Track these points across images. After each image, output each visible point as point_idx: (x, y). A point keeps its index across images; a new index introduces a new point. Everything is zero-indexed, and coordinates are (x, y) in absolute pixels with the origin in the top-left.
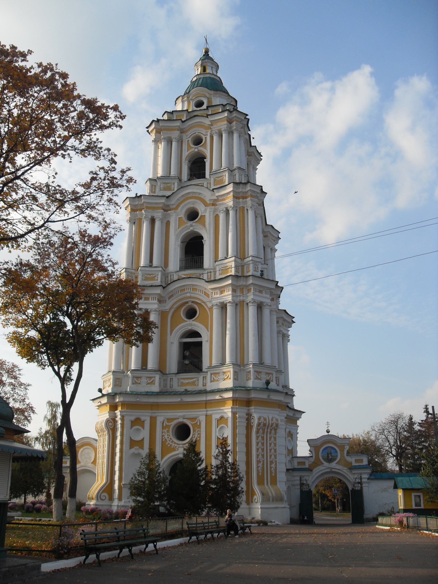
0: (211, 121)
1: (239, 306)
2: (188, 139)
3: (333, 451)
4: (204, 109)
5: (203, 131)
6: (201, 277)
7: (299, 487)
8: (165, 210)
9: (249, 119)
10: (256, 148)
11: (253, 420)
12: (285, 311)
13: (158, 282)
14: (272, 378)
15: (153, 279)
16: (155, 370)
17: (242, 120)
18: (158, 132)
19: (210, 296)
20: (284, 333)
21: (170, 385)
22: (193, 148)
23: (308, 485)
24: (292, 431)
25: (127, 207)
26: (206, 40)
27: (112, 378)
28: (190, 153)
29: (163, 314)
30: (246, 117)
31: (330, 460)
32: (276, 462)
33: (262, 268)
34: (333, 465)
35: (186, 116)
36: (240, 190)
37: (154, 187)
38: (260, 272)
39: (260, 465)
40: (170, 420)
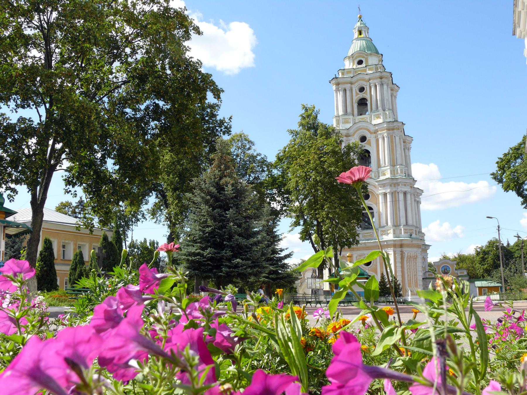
5: (365, 83)
18: (338, 84)
36: (391, 125)
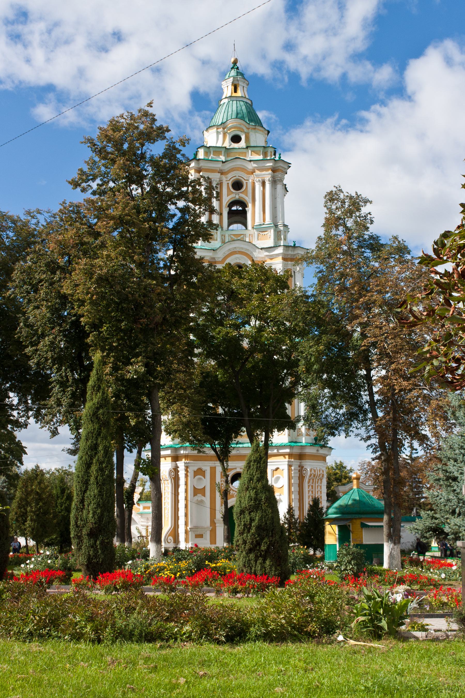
5: (245, 176)
22: (233, 193)
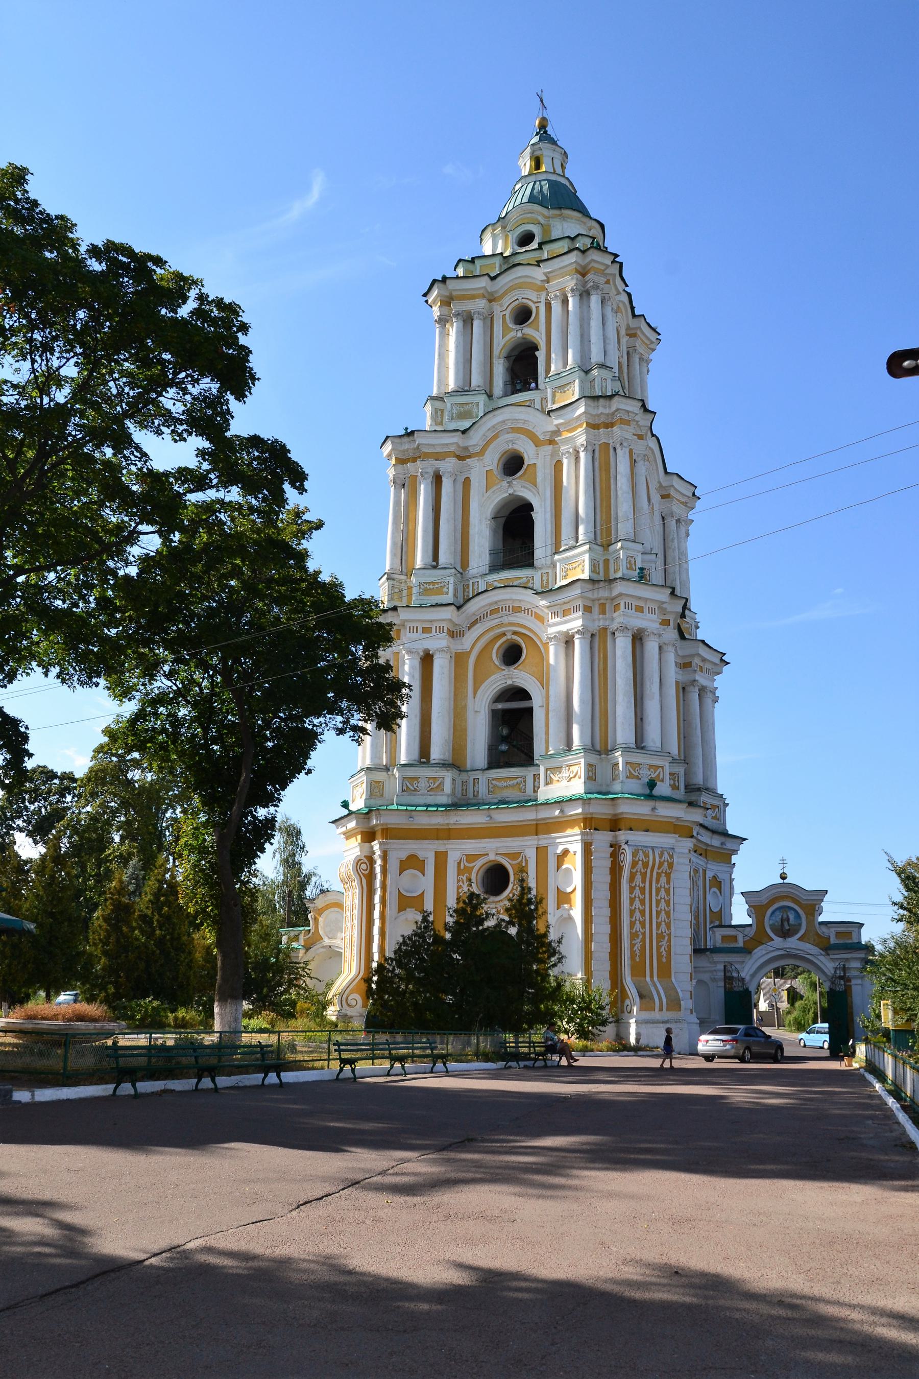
0: (545, 274)
1: (597, 639)
2: (504, 313)
3: (792, 916)
4: (534, 250)
5: (533, 296)
6: (530, 585)
7: (722, 984)
8: (461, 458)
9: (621, 264)
10: (645, 319)
11: (623, 855)
12: (703, 642)
13: (449, 598)
14: (661, 776)
15: (439, 591)
16: (443, 764)
17: (607, 266)
18: (446, 302)
19: (546, 621)
20: (703, 686)
21: (474, 791)
23: (743, 979)
24: (721, 876)
25: (389, 455)
26: (542, 101)
27: (365, 781)
28: (507, 342)
29: (459, 659)
30: (616, 260)
31: (785, 932)
32: (669, 935)
33: (643, 562)
34: (793, 943)
35: (500, 266)
36: (601, 410)
37: (439, 413)
38: (638, 571)
39: (638, 941)
40: (471, 858)
